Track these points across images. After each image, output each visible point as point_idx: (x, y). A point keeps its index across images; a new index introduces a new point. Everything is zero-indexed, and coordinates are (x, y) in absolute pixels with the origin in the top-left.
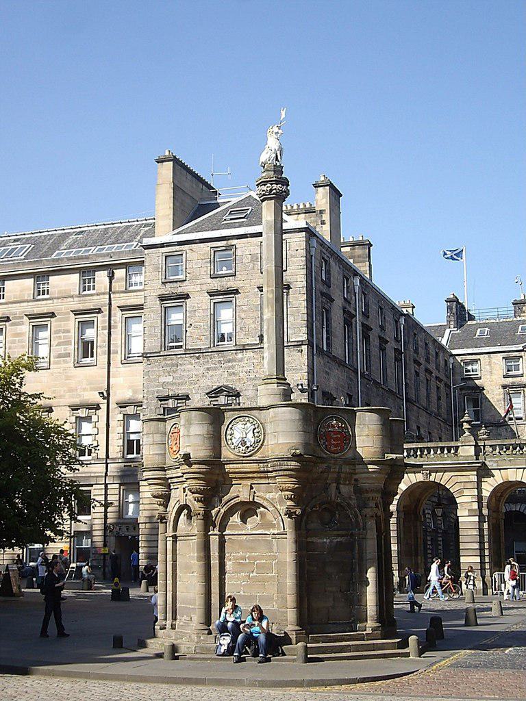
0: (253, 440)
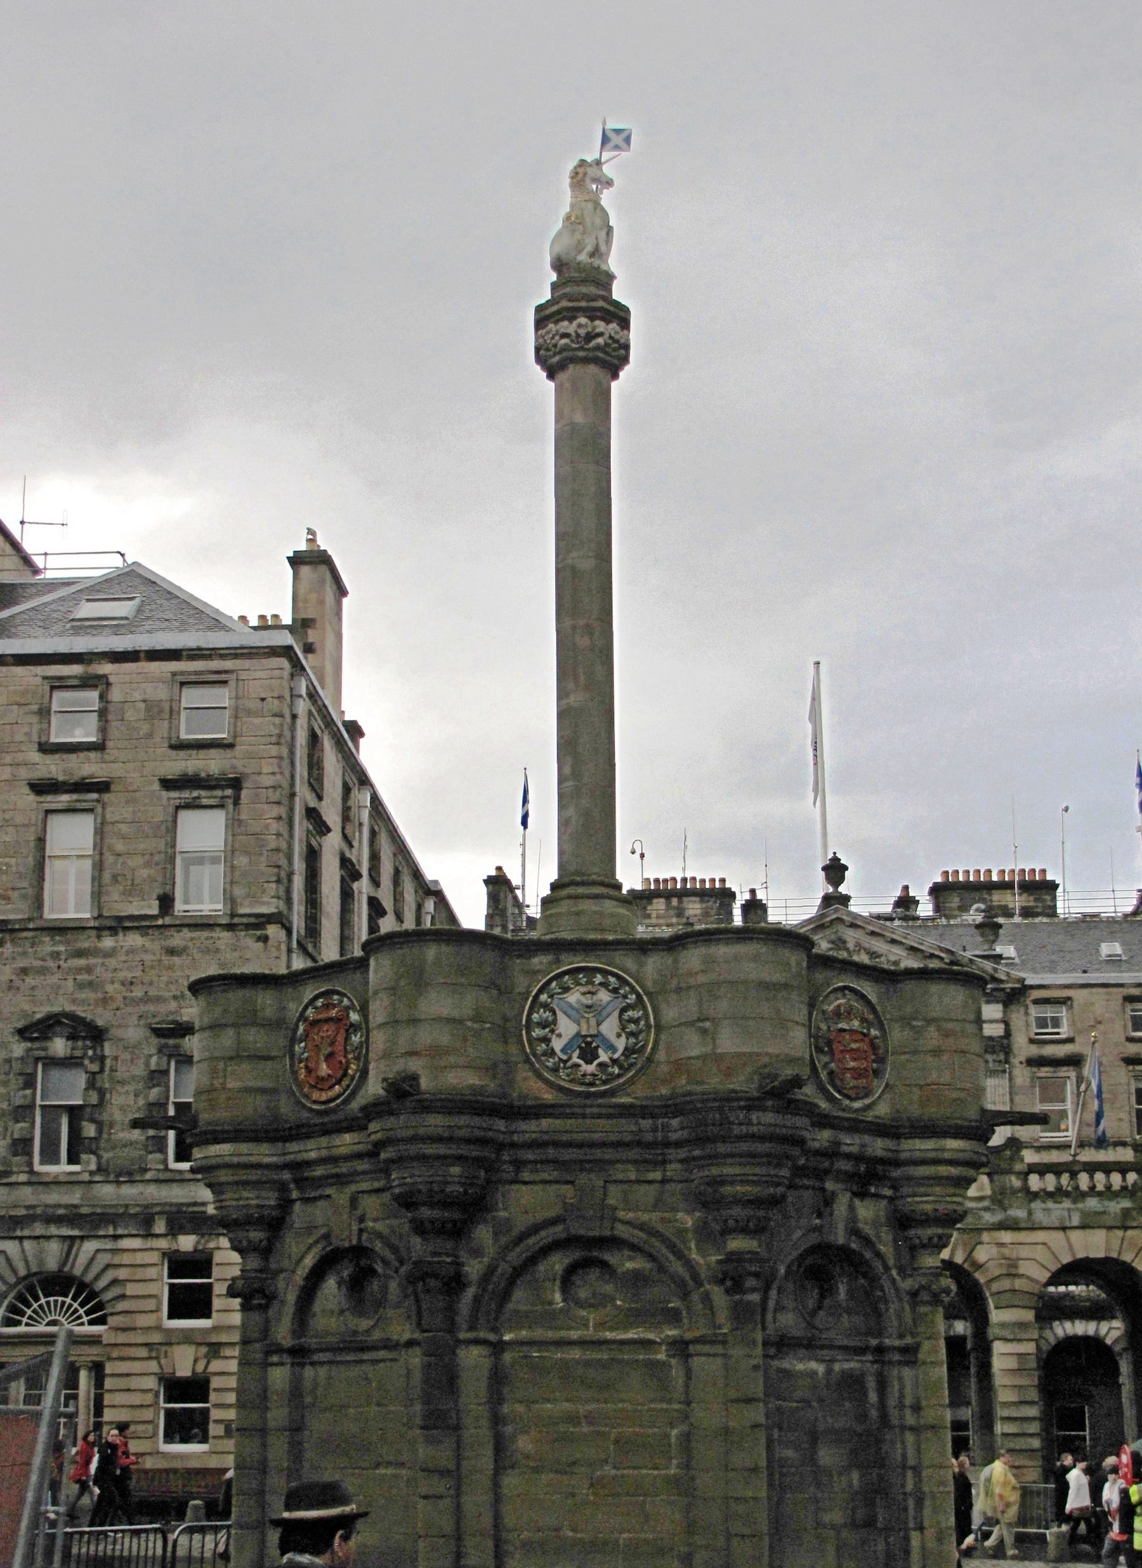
0: (621, 1044)
